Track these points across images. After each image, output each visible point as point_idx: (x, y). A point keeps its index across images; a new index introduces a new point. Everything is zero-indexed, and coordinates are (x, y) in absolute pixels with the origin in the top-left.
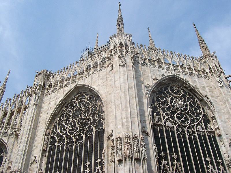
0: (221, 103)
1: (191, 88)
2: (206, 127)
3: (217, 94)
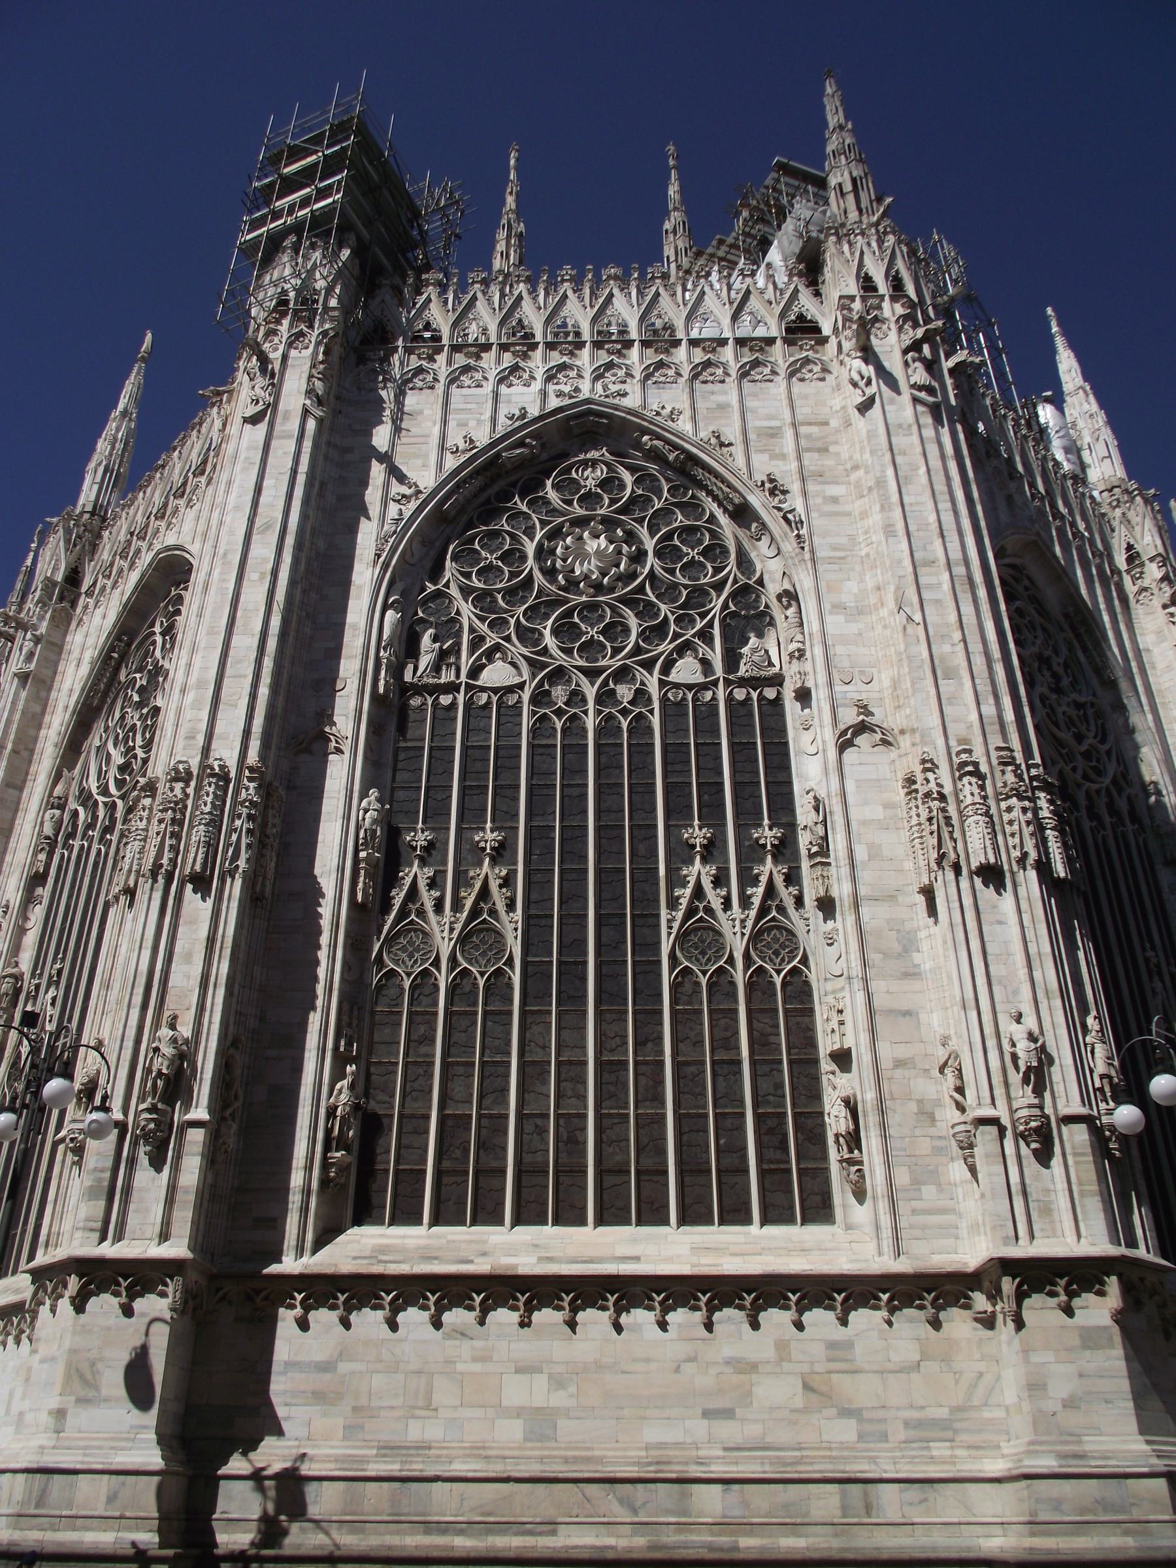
0: (859, 502)
1: (684, 451)
2: (732, 659)
3: (851, 458)
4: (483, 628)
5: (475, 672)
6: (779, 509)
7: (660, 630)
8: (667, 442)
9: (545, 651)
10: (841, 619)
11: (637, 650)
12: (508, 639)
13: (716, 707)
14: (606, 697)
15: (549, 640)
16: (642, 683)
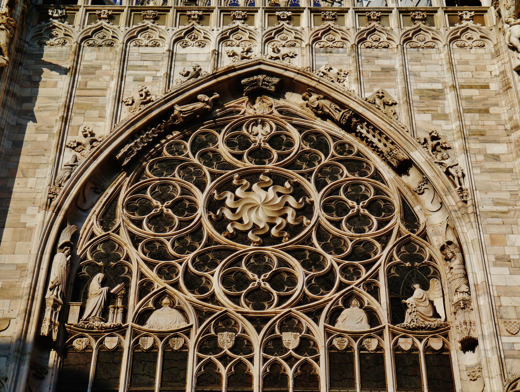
2: (397, 312)
4: (152, 275)
5: (142, 317)
6: (441, 164)
7: (325, 282)
8: (334, 101)
9: (212, 299)
10: (506, 270)
11: (303, 299)
12: (176, 285)
13: (382, 357)
14: (274, 345)
15: (217, 287)
16: (308, 331)
